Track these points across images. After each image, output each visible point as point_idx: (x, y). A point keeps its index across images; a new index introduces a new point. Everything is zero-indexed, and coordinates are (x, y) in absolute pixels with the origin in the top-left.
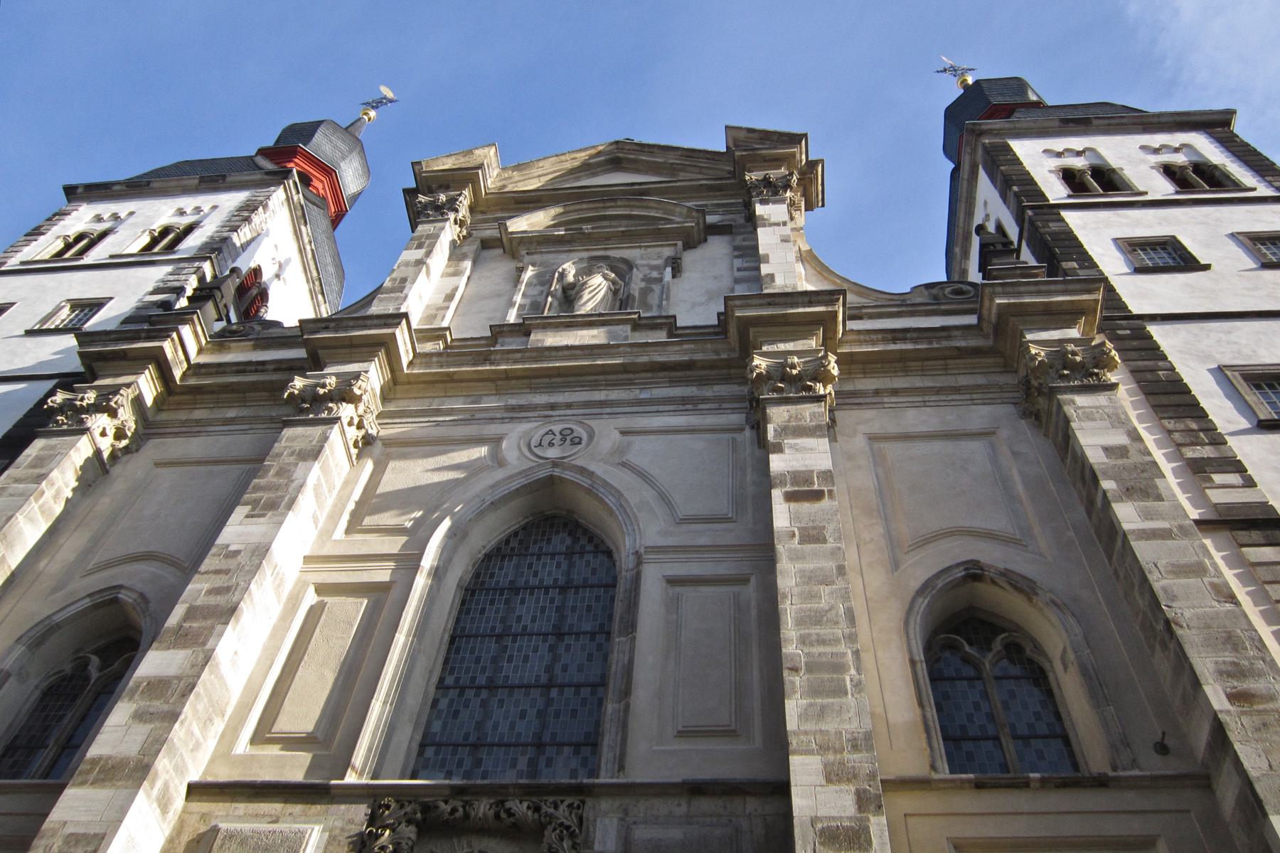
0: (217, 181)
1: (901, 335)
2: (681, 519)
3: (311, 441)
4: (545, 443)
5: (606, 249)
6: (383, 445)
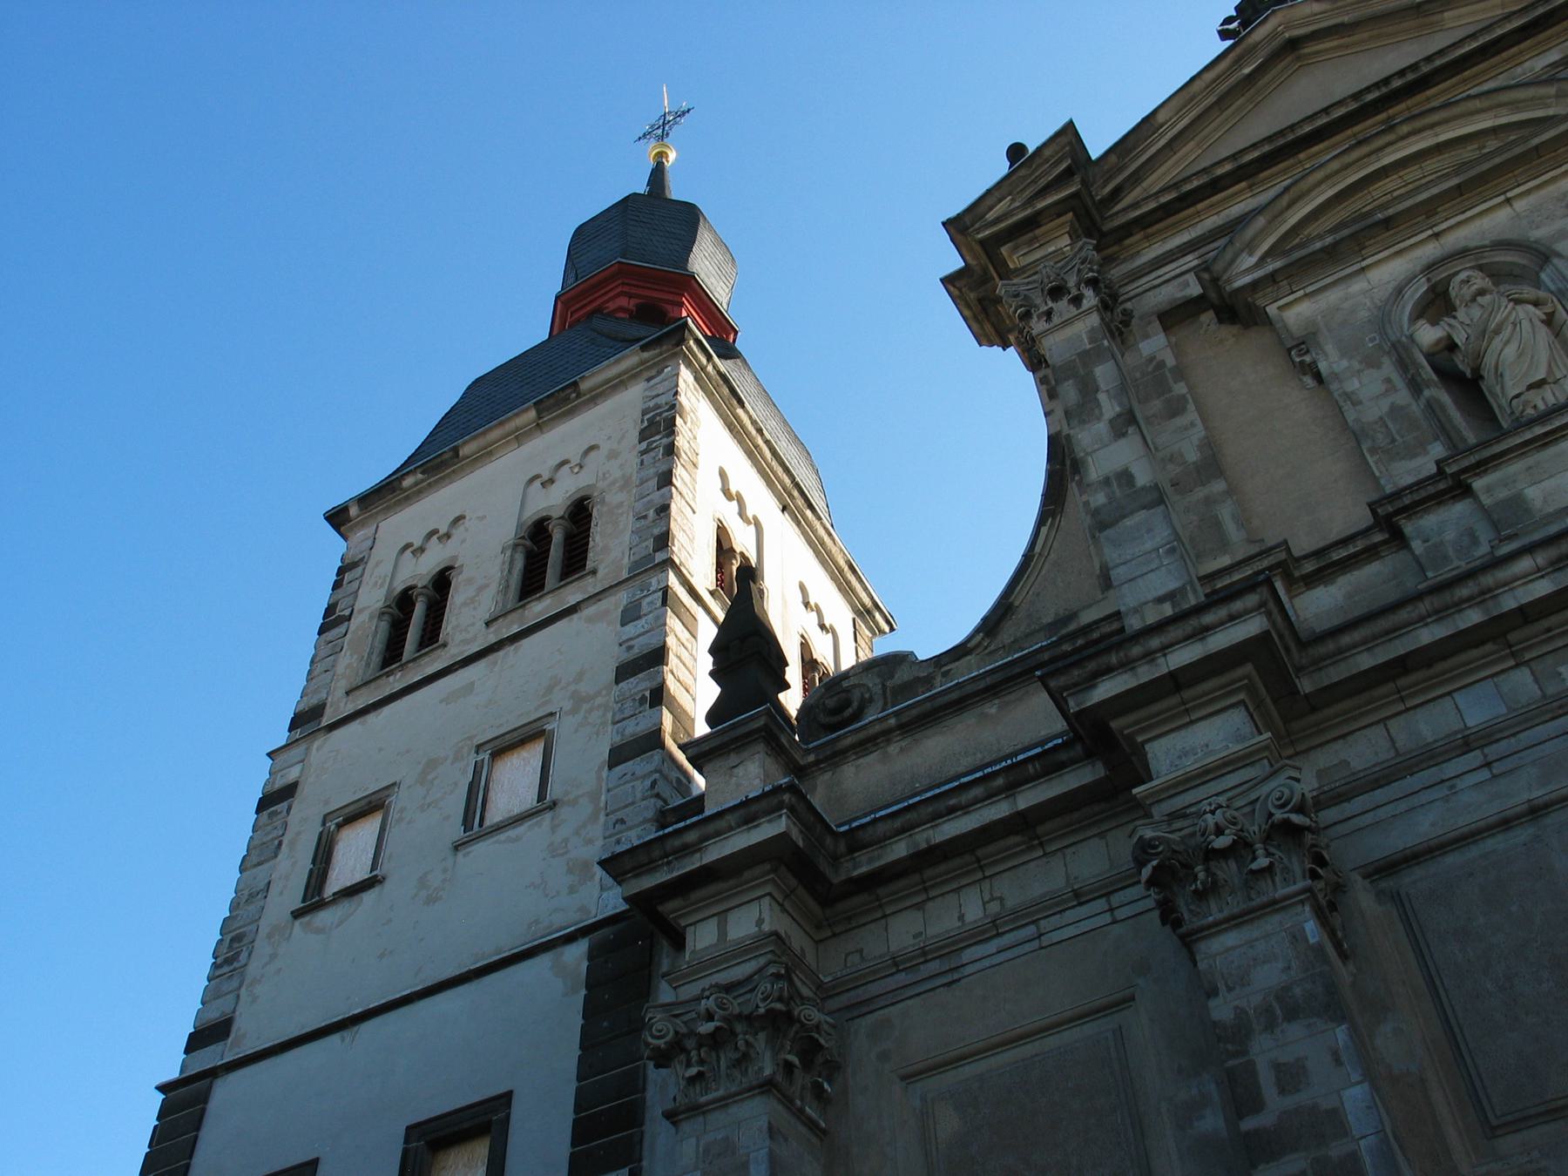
0: (567, 400)
6: (1365, 877)
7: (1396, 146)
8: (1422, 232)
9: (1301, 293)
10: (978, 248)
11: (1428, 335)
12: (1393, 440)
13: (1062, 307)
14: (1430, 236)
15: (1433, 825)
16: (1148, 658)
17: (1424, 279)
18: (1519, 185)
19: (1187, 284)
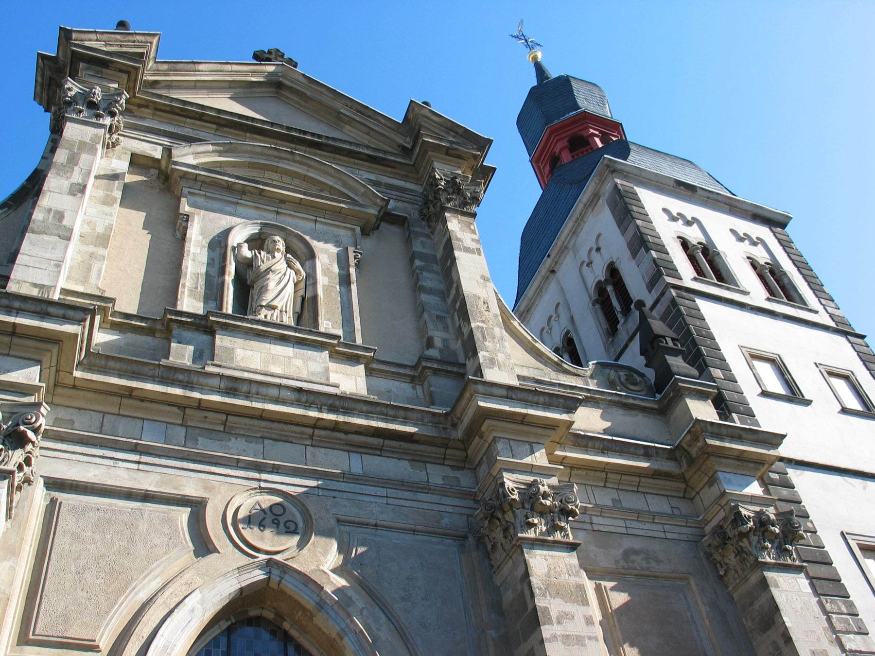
7: (288, 162)
8: (272, 206)
9: (204, 193)
10: (69, 53)
12: (197, 288)
14: (275, 211)
15: (95, 476)
16: (8, 309)
17: (260, 228)
18: (324, 218)
19: (156, 150)
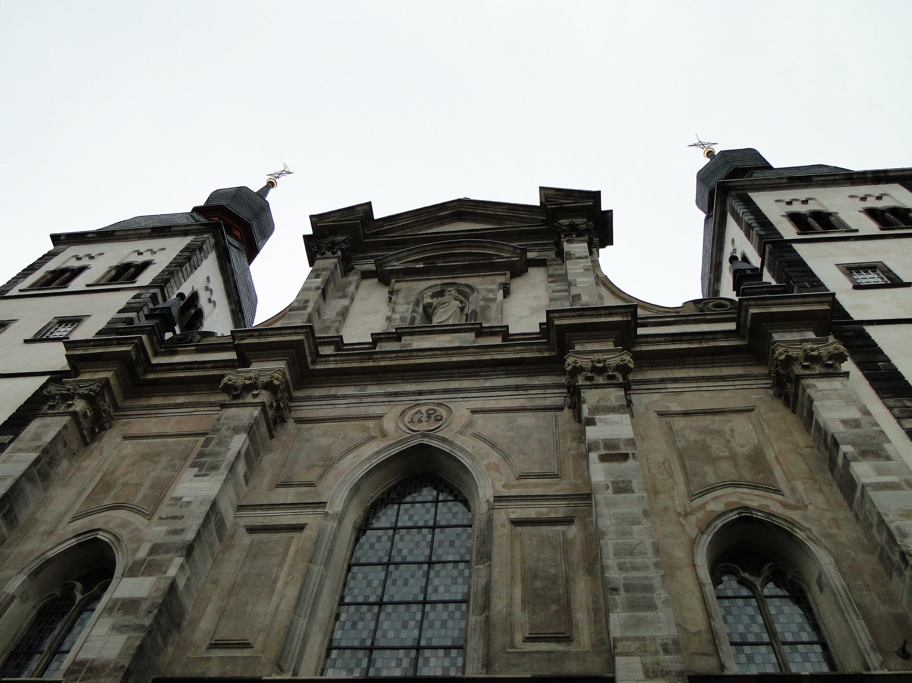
1: (677, 338)
2: (520, 476)
3: (242, 420)
4: (416, 420)
5: (454, 278)
11: (428, 300)
13: (329, 254)
